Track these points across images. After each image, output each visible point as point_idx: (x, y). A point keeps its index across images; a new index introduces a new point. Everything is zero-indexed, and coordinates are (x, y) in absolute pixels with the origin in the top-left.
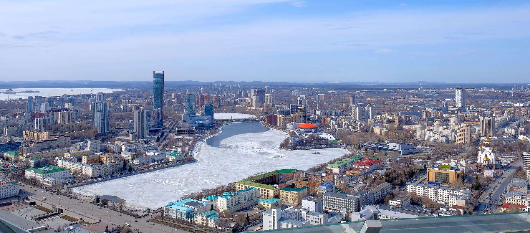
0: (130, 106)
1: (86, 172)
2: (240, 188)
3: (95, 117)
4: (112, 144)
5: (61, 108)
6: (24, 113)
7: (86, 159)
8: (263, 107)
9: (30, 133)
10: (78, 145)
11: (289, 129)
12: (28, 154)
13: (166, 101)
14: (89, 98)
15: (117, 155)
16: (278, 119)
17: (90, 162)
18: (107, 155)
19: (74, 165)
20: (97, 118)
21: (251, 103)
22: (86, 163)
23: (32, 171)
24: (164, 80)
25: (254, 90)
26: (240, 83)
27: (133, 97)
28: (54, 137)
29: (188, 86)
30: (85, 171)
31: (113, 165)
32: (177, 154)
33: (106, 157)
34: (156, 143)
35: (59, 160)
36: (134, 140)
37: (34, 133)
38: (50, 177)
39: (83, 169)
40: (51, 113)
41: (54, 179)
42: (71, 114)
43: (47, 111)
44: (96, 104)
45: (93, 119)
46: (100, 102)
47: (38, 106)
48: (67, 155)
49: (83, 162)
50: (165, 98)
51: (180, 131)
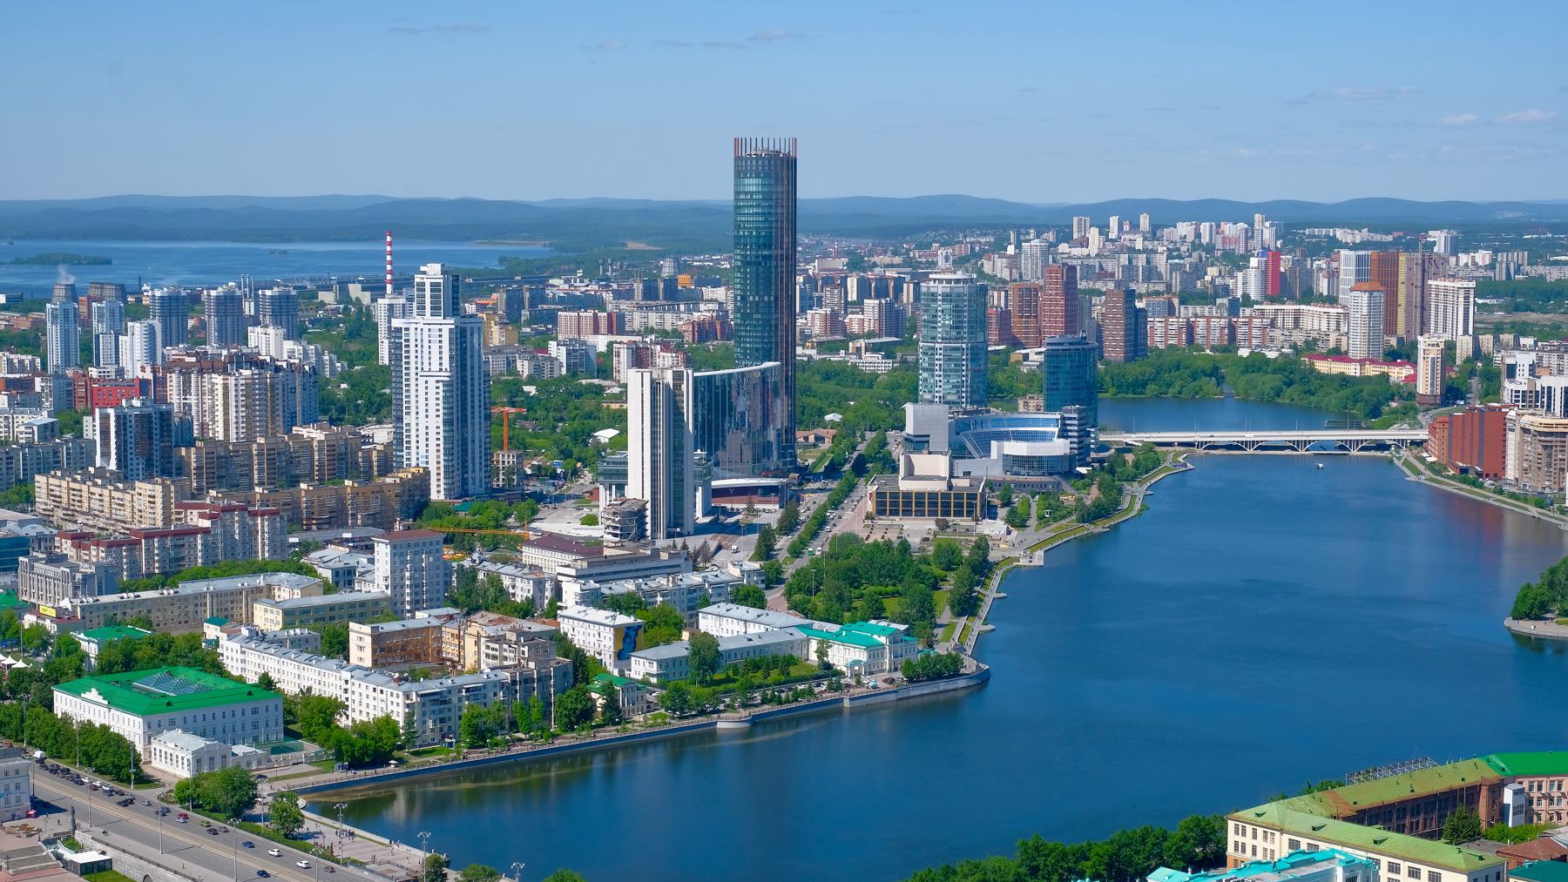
0: (602, 348)
1: (371, 710)
2: (1254, 849)
3: (413, 411)
4: (505, 562)
5: (225, 352)
6: (38, 380)
7: (368, 640)
8: (1414, 364)
9: (69, 489)
12: (65, 603)
13: (812, 321)
14: (374, 300)
16: (1512, 439)
17: (387, 653)
18: (481, 625)
19: (304, 673)
21: (1333, 337)
22: (368, 663)
23: (93, 695)
25: (1359, 258)
26: (1269, 210)
27: (618, 295)
28: (195, 512)
29: (943, 227)
30: (363, 708)
31: (514, 682)
32: (875, 637)
33: (479, 636)
34: (756, 566)
35: (224, 641)
36: (627, 543)
37: (93, 489)
38: (185, 730)
39: (357, 697)
40: (174, 381)
41: (200, 743)
42: (280, 387)
43: (154, 371)
44: (412, 331)
45: (400, 419)
46: (440, 319)
47: (105, 343)
49: (354, 660)
51: (895, 495)
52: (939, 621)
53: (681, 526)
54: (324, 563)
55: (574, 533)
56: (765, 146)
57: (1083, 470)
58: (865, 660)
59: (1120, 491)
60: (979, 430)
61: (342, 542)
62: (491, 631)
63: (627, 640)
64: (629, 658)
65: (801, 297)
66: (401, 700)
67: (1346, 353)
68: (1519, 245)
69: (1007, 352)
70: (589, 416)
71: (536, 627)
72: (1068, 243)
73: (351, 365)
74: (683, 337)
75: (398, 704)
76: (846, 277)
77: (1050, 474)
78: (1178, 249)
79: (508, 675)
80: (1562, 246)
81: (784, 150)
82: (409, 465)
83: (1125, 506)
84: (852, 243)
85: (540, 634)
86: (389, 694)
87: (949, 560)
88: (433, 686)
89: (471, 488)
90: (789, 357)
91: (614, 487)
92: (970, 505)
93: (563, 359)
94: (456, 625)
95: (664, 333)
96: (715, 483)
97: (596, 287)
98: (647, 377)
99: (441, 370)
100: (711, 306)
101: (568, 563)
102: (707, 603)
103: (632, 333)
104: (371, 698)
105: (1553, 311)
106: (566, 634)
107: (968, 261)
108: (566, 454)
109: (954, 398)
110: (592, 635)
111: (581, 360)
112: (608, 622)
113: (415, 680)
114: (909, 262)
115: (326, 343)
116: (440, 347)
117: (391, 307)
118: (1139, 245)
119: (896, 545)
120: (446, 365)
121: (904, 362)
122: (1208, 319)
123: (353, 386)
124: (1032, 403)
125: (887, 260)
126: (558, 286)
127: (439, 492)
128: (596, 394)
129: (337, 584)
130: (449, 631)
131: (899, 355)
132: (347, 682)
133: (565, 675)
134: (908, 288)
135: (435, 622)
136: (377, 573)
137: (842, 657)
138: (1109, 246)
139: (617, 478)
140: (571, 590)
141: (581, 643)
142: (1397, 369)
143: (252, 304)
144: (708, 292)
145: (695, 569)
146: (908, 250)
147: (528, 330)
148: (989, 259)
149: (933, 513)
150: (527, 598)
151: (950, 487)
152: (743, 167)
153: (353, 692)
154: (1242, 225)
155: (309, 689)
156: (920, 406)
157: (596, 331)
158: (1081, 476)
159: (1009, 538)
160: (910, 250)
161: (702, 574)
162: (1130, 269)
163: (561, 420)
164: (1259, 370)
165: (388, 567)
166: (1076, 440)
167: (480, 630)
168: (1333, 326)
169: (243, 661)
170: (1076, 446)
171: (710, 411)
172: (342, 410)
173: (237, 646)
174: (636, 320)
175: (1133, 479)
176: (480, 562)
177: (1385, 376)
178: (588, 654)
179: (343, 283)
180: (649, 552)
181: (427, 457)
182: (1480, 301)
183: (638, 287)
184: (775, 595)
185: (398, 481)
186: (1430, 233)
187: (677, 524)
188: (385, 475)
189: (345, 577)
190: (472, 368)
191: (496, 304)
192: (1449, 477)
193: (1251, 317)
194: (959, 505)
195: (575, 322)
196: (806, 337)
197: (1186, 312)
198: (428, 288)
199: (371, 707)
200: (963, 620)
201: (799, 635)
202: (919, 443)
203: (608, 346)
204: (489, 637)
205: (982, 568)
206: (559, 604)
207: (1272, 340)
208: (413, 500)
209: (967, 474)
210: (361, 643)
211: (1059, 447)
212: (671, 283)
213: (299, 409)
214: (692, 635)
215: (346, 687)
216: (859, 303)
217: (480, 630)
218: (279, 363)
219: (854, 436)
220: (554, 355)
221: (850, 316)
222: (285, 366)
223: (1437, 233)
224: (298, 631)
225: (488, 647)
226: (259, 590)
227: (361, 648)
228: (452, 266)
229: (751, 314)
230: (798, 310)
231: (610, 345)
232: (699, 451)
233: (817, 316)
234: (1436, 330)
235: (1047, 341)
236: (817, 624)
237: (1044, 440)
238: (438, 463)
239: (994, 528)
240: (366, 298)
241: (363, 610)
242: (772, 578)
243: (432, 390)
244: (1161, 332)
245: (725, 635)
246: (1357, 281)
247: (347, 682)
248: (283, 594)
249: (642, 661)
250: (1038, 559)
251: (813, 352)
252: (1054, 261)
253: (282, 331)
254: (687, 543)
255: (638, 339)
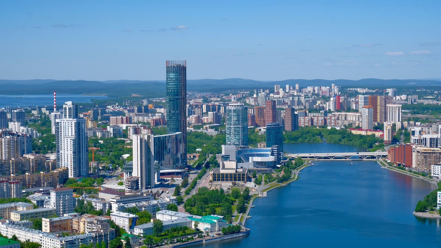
0: (124, 128)
3: (63, 149)
4: (93, 198)
7: (48, 224)
8: (383, 131)
10: (34, 199)
11: (437, 176)
13: (192, 119)
14: (50, 113)
15: (103, 218)
16: (414, 154)
18: (85, 218)
20: (66, 150)
21: (357, 123)
24: (188, 78)
25: (365, 97)
26: (337, 82)
27: (129, 111)
29: (233, 88)
31: (96, 237)
32: (213, 220)
33: (85, 222)
34: (175, 198)
36: (133, 191)
39: (44, 242)
42: (19, 141)
44: (62, 123)
45: (59, 152)
46: (71, 119)
48: (16, 216)
49: (44, 230)
50: (190, 113)
51: (219, 175)
52: (233, 215)
53: (150, 185)
54: (34, 199)
55: (115, 188)
56: (176, 63)
57: (279, 166)
58: (210, 228)
59: (291, 172)
60: (245, 153)
61: (40, 192)
62: (89, 220)
63: (133, 222)
64: (134, 228)
65: (188, 112)
66: (59, 243)
67: (362, 128)
68: (415, 93)
69: (254, 129)
70: (120, 150)
71: (103, 218)
72: (273, 93)
73: (43, 134)
74: (150, 124)
75: (58, 244)
76: (202, 105)
77: (268, 167)
78: (308, 95)
79: (94, 234)
80: (428, 93)
81: (182, 64)
82: (62, 167)
83: (292, 177)
84: (204, 94)
85: (105, 221)
86: (55, 241)
87: (236, 195)
88: (69, 238)
89: (82, 174)
90: (184, 131)
91: (128, 173)
92: (243, 177)
93: (112, 132)
94: (77, 218)
95: (144, 123)
96: (161, 171)
97: (122, 109)
98: (139, 137)
99: (72, 136)
100: (159, 114)
101: (114, 197)
102: (159, 210)
103: (134, 123)
104: (49, 242)
105: (426, 114)
106: (113, 221)
107: (241, 99)
108: (113, 162)
109: (237, 143)
110: (121, 221)
111: (118, 132)
112: (127, 216)
113: (64, 236)
114: (222, 100)
115: (35, 127)
116: (72, 128)
117: (55, 115)
118: (295, 94)
119: (219, 191)
120: (74, 134)
121: (221, 132)
122: (318, 117)
123: (43, 141)
124: (262, 145)
125: (215, 99)
126: (110, 108)
127: (71, 175)
128: (123, 143)
129: (38, 205)
130: (75, 220)
131: (220, 130)
132: (41, 237)
133: (113, 234)
134: (222, 108)
135: (70, 217)
136: (51, 202)
137: (202, 227)
138: (286, 94)
139: (130, 170)
140: (115, 206)
141: (118, 223)
142: (377, 133)
143: (10, 115)
144: (158, 110)
145: (155, 199)
146: (222, 96)
147: (100, 122)
148: (248, 99)
149: (231, 180)
150: (100, 209)
151: (236, 172)
152: (169, 70)
153: (43, 241)
154: (328, 87)
155: (29, 240)
156: (226, 146)
157: (122, 123)
158: (278, 168)
159: (255, 188)
160: (223, 96)
161: (157, 201)
162: (293, 101)
163: (111, 151)
164: (334, 133)
165: (55, 200)
166: (276, 156)
167: (85, 220)
168: (357, 119)
169: (7, 231)
170: (276, 158)
171: (159, 148)
172: (40, 149)
173: (5, 226)
174: (135, 119)
175: (295, 169)
176: (85, 198)
177: (374, 135)
178: (120, 227)
179: (40, 108)
180: (140, 194)
181: (67, 164)
182: (403, 111)
183: (136, 108)
184: (181, 207)
185: (58, 172)
186: (387, 89)
187: (149, 184)
188: (54, 170)
189: (41, 203)
190: (82, 135)
191: (90, 114)
192: (394, 167)
193: (331, 117)
194: (239, 177)
195: (115, 120)
196: (190, 124)
197: (311, 115)
198: (67, 109)
199: (49, 245)
200: (241, 214)
201: (189, 220)
202: (226, 158)
203: (126, 128)
204: (88, 222)
205: (247, 197)
206: (111, 211)
207: (338, 124)
208: (63, 178)
209: (242, 167)
210: (46, 225)
211: (271, 159)
212: (146, 107)
213: (25, 149)
214: (154, 220)
215: (41, 239)
216: (207, 113)
217: (85, 220)
218: (19, 134)
219: (206, 155)
220: (109, 130)
221: (204, 117)
222: (21, 134)
223: (389, 90)
224: (25, 221)
225: (88, 225)
226: (12, 208)
227: (46, 226)
228: (75, 102)
229: (172, 117)
230: (187, 115)
231: (127, 127)
232: (156, 161)
233: (193, 117)
234: (389, 120)
235: (267, 125)
236: (194, 216)
237: (266, 156)
238: (71, 166)
239: (251, 185)
240: (47, 112)
241: (47, 214)
242: (180, 202)
243: (69, 142)
244: (303, 122)
245: (165, 220)
246: (365, 105)
247: (41, 237)
248: (20, 209)
249: (138, 229)
250: (265, 194)
251: (192, 129)
252: (269, 99)
253: (20, 123)
254: (152, 191)
255: (136, 125)
